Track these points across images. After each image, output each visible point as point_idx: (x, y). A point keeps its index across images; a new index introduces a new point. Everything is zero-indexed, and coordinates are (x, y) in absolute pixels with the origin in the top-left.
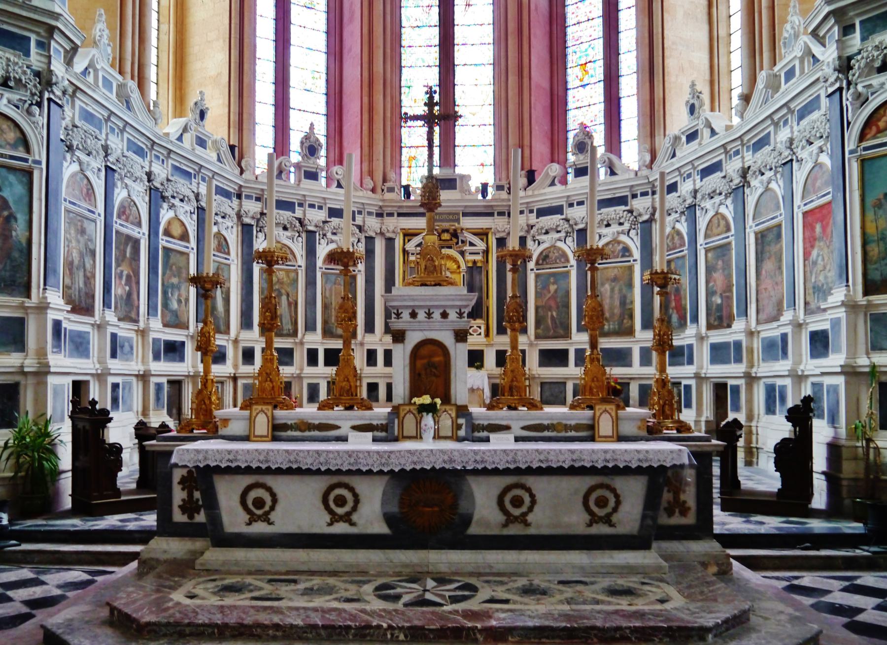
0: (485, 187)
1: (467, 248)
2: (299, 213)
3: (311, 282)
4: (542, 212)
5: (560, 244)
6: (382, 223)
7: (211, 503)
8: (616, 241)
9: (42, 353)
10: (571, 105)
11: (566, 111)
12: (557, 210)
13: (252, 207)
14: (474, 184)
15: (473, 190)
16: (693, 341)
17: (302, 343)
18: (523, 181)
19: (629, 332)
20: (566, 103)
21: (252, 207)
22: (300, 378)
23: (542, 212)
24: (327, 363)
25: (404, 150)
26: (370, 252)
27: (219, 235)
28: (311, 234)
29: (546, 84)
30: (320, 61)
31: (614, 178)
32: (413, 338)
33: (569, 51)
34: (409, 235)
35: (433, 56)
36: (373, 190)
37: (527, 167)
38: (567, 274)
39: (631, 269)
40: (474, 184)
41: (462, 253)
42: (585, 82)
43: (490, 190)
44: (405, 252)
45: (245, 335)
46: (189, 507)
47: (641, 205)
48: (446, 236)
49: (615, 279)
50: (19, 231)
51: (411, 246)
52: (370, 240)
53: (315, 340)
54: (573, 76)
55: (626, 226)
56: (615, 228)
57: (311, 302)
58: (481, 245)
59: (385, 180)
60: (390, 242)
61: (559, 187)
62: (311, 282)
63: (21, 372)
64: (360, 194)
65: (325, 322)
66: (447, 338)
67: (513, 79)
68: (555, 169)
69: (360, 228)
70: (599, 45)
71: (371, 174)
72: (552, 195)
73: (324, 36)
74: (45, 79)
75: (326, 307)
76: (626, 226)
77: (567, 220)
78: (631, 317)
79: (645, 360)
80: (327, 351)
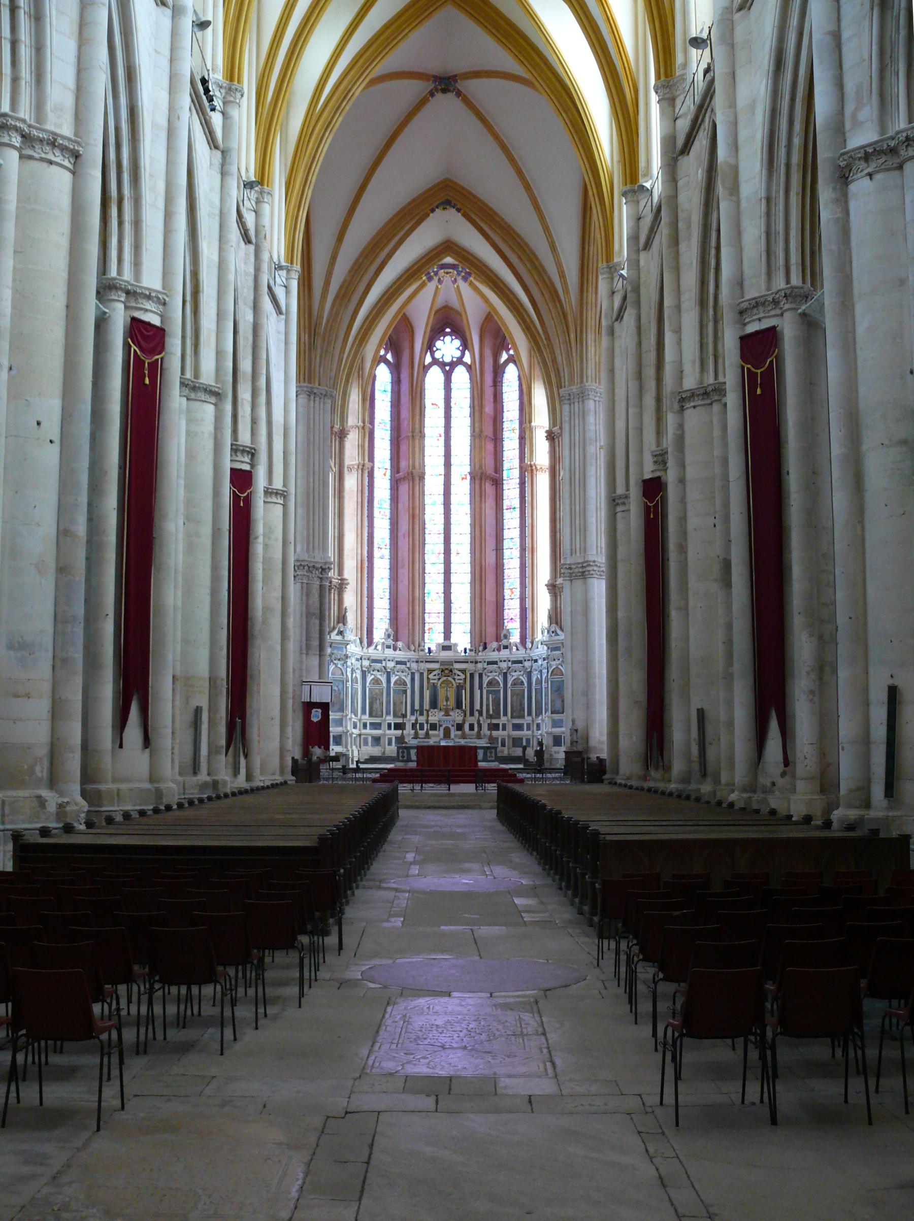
0: (465, 650)
1: (456, 677)
2: (384, 664)
3: (388, 694)
4: (489, 663)
5: (496, 678)
6: (418, 666)
7: (409, 754)
8: (518, 679)
9: (346, 727)
10: (506, 607)
11: (503, 610)
12: (495, 663)
13: (366, 663)
14: (460, 648)
15: (459, 651)
16: (540, 721)
17: (385, 720)
18: (481, 648)
19: (523, 717)
20: (504, 606)
21: (366, 663)
22: (384, 735)
23: (489, 663)
24: (395, 729)
25: (426, 625)
26: (413, 680)
27: (356, 677)
28: (388, 673)
29: (494, 599)
30: (386, 583)
31: (518, 652)
32: (444, 726)
33: (506, 581)
34: (430, 671)
35: (441, 578)
36: (414, 651)
37: (484, 641)
38: (499, 691)
39: (524, 690)
40: (460, 648)
41: (454, 679)
42: (513, 597)
43: (468, 651)
44: (428, 678)
45: (363, 717)
46: (403, 757)
47: (527, 664)
48: (447, 672)
49: (518, 695)
50: (342, 697)
51: (431, 676)
52: (413, 674)
53: (390, 719)
54: (507, 593)
55: (522, 673)
56: (518, 673)
57: (388, 702)
58: (463, 676)
59: (419, 646)
60: (422, 674)
61: (496, 653)
62: (388, 694)
63: (343, 732)
64: (408, 653)
65: (394, 711)
66: (450, 726)
67: (477, 601)
68: (495, 645)
69: (408, 668)
70: (518, 581)
71: (413, 643)
72: (493, 656)
73: (388, 571)
74: (347, 657)
75: (394, 704)
76: (522, 673)
77: (499, 668)
78: (524, 711)
79: (528, 729)
80: (395, 724)
